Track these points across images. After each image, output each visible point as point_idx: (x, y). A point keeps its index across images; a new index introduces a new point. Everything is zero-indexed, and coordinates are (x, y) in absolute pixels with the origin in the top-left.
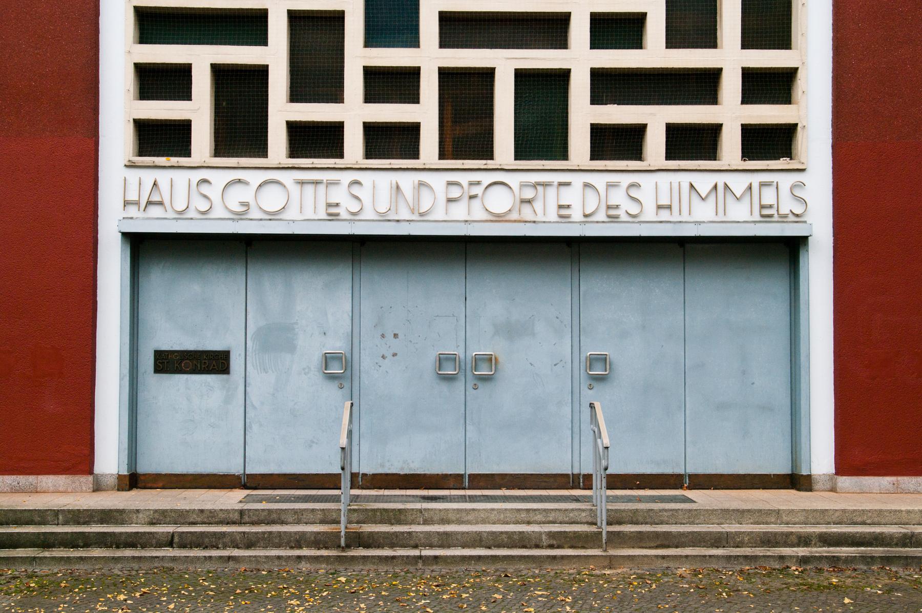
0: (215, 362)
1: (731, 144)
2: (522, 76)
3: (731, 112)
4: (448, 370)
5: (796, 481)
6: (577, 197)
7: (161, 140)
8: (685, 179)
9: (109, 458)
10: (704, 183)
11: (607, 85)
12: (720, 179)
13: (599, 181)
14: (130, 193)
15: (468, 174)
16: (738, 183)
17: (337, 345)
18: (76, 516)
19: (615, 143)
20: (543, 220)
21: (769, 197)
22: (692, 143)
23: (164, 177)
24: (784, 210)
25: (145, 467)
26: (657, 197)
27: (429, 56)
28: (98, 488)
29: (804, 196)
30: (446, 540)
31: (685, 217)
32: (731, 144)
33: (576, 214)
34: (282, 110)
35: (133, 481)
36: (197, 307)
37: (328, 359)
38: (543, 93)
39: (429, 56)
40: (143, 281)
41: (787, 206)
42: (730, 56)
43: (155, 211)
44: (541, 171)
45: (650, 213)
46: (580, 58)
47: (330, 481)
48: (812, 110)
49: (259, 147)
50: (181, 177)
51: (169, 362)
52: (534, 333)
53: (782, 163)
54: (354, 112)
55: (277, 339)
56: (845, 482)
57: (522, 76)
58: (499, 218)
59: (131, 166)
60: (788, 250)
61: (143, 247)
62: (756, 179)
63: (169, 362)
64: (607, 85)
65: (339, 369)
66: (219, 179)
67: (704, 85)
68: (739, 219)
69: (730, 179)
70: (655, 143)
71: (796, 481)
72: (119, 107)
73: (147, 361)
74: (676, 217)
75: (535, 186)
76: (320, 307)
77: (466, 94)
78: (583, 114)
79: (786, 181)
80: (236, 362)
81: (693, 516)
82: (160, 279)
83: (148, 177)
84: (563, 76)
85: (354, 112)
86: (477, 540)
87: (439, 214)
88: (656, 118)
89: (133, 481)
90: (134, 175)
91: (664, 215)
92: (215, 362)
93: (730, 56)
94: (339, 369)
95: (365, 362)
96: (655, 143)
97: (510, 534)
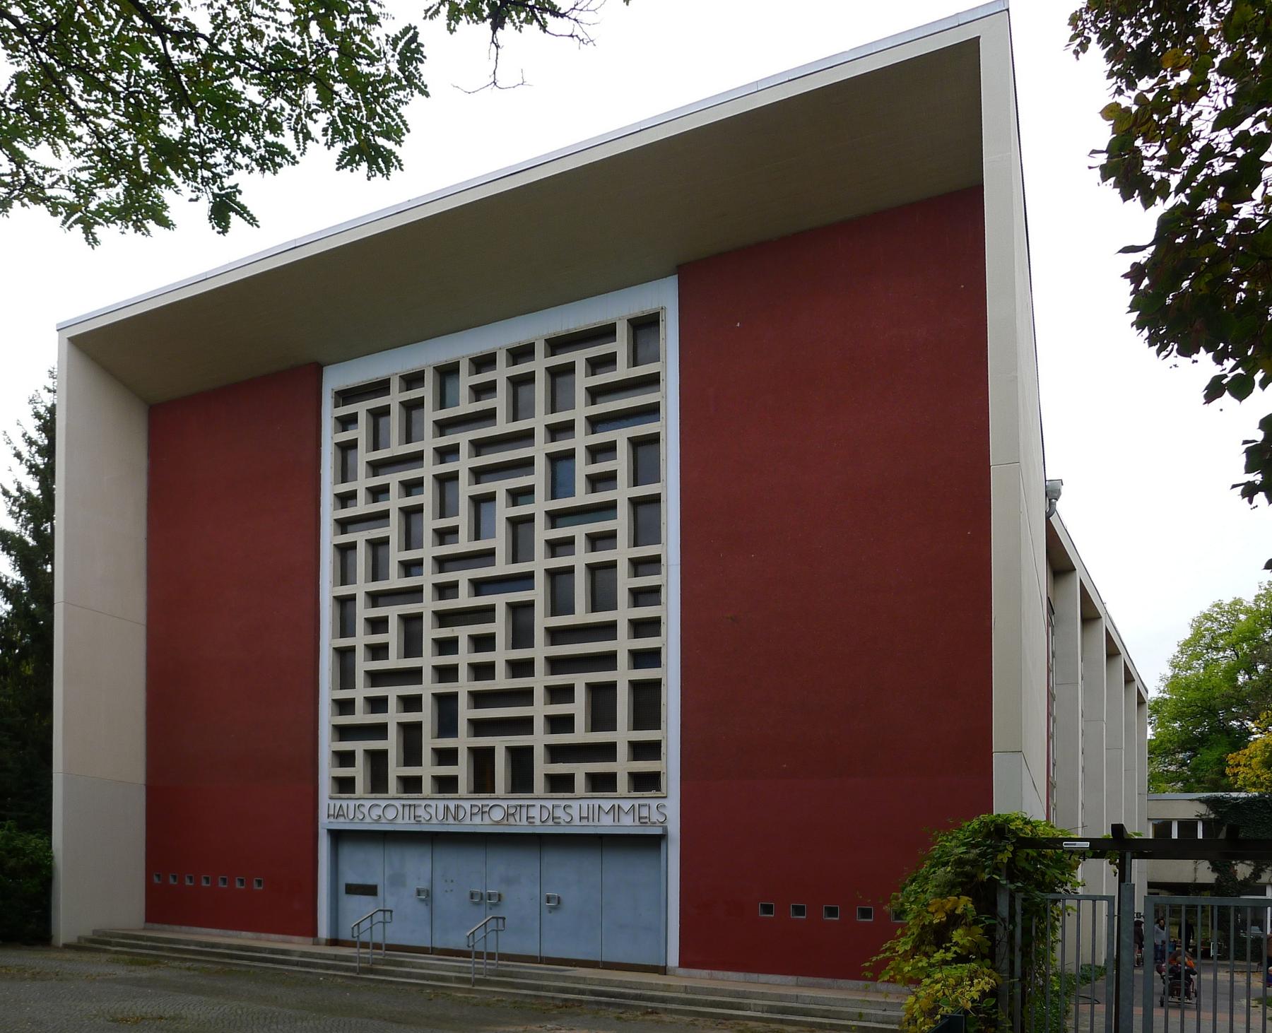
0: (370, 890)
1: (623, 783)
2: (510, 750)
3: (623, 766)
4: (478, 899)
5: (662, 970)
6: (540, 812)
7: (345, 785)
8: (596, 803)
9: (324, 931)
10: (607, 805)
11: (556, 753)
12: (616, 802)
13: (549, 804)
14: (331, 811)
15: (483, 800)
16: (626, 805)
17: (424, 885)
18: (273, 951)
19: (561, 784)
20: (520, 825)
21: (644, 813)
22: (602, 783)
23: (344, 803)
24: (654, 819)
25: (345, 934)
26: (579, 812)
27: (463, 741)
28: (317, 943)
29: (666, 812)
30: (409, 975)
31: (596, 823)
32: (623, 783)
33: (537, 822)
34: (395, 769)
35: (334, 942)
36: (364, 865)
37: (419, 892)
38: (521, 757)
39: (463, 741)
40: (340, 851)
41: (656, 817)
42: (623, 735)
43: (341, 819)
44: (521, 799)
45: (576, 821)
46: (539, 739)
47: (466, 954)
48: (670, 765)
49: (384, 789)
50: (352, 804)
51: (353, 889)
52: (520, 882)
53: (653, 793)
54: (428, 770)
55: (398, 881)
56: (682, 971)
57: (510, 750)
58: (498, 823)
59: (331, 798)
60: (653, 843)
61: (338, 837)
62: (637, 803)
63: (353, 889)
64: (556, 753)
65: (426, 896)
66: (368, 804)
67: (607, 751)
68: (628, 824)
69: (621, 802)
70: (580, 783)
71: (662, 970)
72: (327, 771)
73: (342, 889)
74: (591, 823)
75: (516, 807)
76: (417, 867)
77: (482, 759)
78: (541, 768)
79: (654, 803)
80: (380, 890)
81: (565, 978)
82: (347, 851)
83: (338, 803)
84: (530, 750)
85: (428, 770)
86: (423, 977)
87: (468, 821)
88: (580, 770)
89: (334, 942)
90: (332, 803)
91: (585, 822)
92: (370, 890)
93: (623, 735)
94: (426, 896)
95: (438, 892)
96: (580, 783)
97: (784, 1007)
